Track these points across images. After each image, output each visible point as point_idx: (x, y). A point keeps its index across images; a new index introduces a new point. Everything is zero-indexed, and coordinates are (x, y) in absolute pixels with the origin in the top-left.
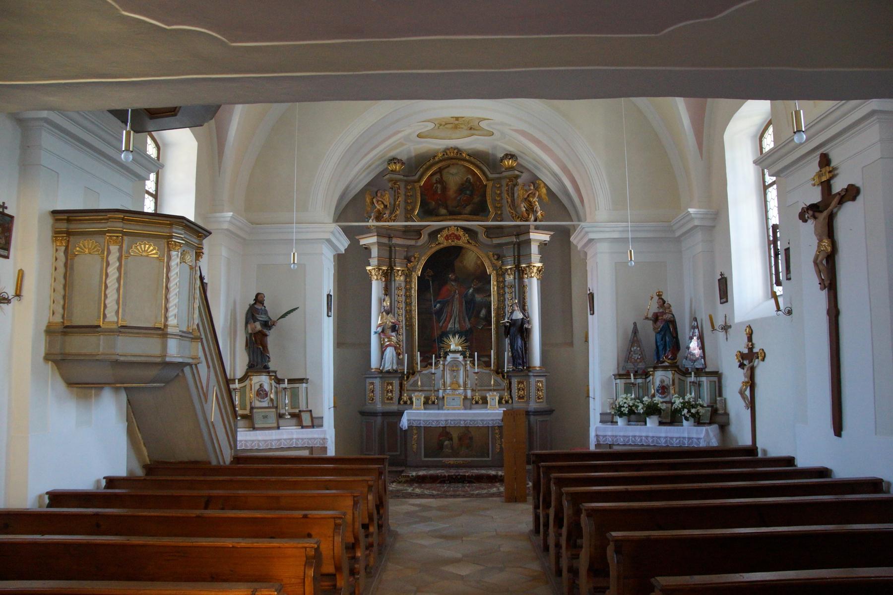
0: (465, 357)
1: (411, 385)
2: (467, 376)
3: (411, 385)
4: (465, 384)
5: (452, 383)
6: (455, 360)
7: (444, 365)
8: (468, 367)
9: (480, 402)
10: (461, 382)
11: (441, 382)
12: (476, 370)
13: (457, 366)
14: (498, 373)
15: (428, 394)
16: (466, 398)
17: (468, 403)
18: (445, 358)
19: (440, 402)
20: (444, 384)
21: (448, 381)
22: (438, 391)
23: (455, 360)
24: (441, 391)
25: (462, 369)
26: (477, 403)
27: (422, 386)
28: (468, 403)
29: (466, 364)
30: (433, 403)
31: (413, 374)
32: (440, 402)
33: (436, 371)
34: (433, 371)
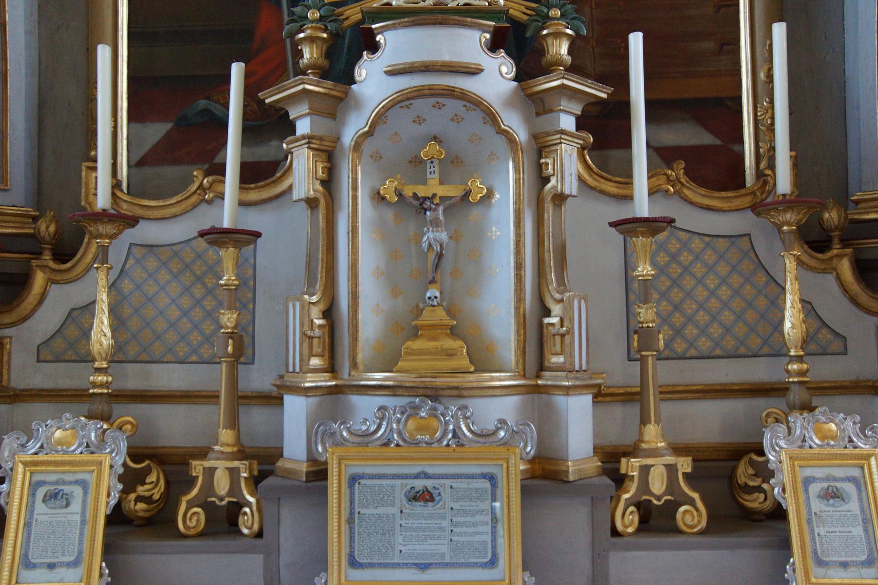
0: (529, 62)
1: (45, 353)
2: (548, 261)
3: (45, 353)
4: (537, 339)
5: (408, 327)
6: (435, 87)
7: (328, 153)
8: (568, 164)
9: (692, 516)
10: (498, 309)
11: (302, 315)
12: (642, 206)
13: (453, 164)
14: (816, 241)
15: (174, 426)
16: (545, 475)
17: (571, 523)
18: (339, 68)
19: (290, 523)
20: (332, 336)
21: (371, 313)
22: (273, 400)
23: (435, 87)
24: (296, 410)
25: (507, 183)
26: (656, 520)
27: (118, 356)
28: (571, 524)
29: (542, 146)
30: (224, 521)
31: (65, 251)
32: (290, 523)
33: (252, 220)
34: (227, 215)
